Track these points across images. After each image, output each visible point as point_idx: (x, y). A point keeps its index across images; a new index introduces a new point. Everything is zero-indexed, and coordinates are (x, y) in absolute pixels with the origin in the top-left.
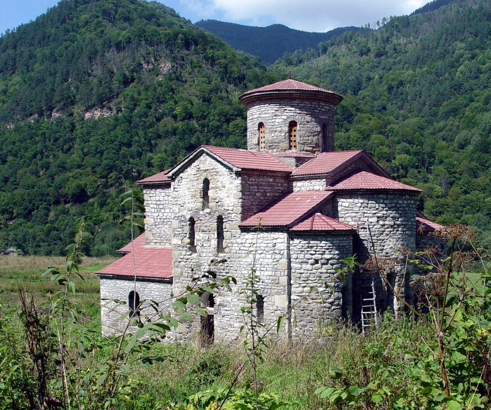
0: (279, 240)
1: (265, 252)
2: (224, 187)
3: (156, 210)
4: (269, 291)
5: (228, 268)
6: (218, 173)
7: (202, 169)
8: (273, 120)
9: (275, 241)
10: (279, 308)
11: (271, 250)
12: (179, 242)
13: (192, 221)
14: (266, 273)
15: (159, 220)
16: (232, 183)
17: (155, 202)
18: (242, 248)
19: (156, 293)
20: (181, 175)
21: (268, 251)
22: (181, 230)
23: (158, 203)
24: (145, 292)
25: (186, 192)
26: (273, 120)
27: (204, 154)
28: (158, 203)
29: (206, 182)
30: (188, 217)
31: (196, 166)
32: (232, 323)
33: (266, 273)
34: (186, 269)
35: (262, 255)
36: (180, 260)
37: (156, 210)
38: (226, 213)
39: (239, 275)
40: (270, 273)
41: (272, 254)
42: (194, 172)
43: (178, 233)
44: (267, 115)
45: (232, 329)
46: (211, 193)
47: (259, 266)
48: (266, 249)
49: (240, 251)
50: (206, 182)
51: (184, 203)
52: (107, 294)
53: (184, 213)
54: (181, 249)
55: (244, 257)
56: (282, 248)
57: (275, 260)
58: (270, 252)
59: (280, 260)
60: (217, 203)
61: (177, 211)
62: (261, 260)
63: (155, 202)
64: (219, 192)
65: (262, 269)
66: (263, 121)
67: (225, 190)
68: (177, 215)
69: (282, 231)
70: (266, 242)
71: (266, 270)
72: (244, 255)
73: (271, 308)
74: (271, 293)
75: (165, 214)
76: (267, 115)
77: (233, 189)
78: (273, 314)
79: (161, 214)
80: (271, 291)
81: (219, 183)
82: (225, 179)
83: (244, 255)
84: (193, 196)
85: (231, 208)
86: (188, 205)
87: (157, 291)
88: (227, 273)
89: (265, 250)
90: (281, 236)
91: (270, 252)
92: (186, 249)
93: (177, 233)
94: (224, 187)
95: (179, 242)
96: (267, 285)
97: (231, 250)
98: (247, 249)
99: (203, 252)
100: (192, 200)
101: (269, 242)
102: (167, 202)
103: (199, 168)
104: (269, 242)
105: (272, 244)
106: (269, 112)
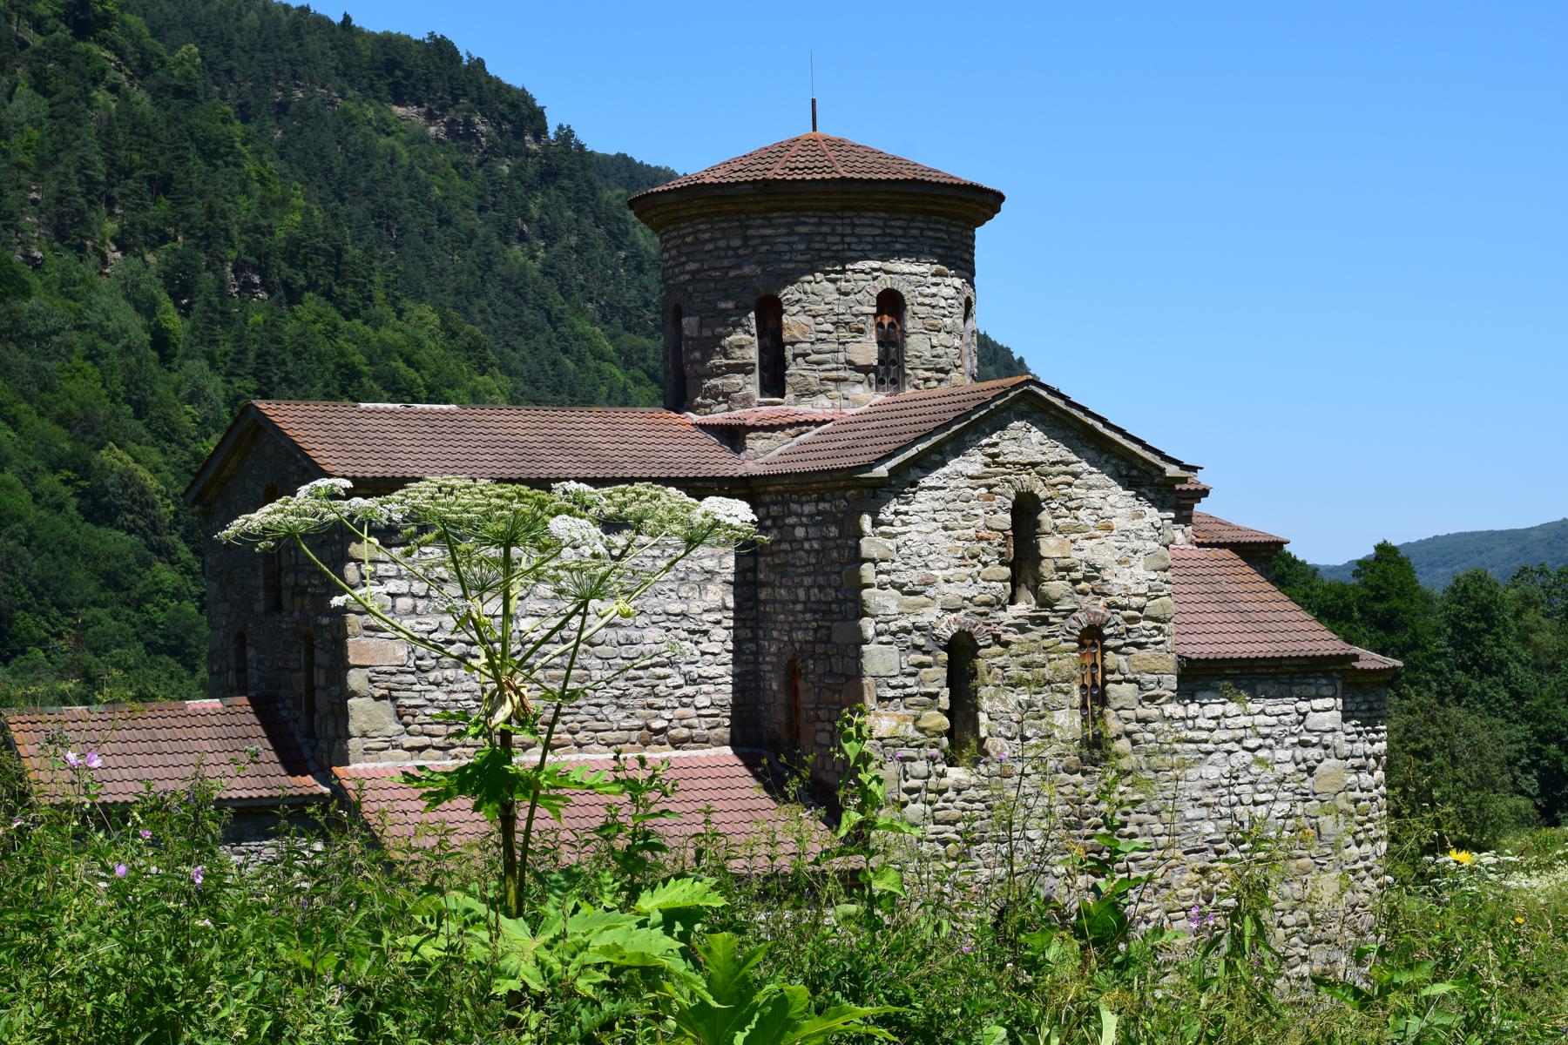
1: (1270, 741)
2: (1109, 528)
7: (1011, 458)
8: (934, 290)
13: (961, 654)
22: (910, 681)
25: (939, 537)
26: (934, 290)
30: (947, 627)
36: (904, 797)
46: (1049, 547)
47: (1249, 788)
50: (1026, 510)
53: (929, 615)
56: (1328, 726)
58: (1288, 741)
59: (1321, 767)
60: (1075, 582)
62: (1254, 769)
65: (1259, 797)
66: (903, 288)
68: (893, 627)
77: (1146, 534)
81: (1081, 514)
82: (1110, 499)
85: (1137, 601)
86: (945, 588)
91: (1288, 741)
93: (890, 693)
98: (1205, 735)
100: (968, 571)
103: (997, 455)
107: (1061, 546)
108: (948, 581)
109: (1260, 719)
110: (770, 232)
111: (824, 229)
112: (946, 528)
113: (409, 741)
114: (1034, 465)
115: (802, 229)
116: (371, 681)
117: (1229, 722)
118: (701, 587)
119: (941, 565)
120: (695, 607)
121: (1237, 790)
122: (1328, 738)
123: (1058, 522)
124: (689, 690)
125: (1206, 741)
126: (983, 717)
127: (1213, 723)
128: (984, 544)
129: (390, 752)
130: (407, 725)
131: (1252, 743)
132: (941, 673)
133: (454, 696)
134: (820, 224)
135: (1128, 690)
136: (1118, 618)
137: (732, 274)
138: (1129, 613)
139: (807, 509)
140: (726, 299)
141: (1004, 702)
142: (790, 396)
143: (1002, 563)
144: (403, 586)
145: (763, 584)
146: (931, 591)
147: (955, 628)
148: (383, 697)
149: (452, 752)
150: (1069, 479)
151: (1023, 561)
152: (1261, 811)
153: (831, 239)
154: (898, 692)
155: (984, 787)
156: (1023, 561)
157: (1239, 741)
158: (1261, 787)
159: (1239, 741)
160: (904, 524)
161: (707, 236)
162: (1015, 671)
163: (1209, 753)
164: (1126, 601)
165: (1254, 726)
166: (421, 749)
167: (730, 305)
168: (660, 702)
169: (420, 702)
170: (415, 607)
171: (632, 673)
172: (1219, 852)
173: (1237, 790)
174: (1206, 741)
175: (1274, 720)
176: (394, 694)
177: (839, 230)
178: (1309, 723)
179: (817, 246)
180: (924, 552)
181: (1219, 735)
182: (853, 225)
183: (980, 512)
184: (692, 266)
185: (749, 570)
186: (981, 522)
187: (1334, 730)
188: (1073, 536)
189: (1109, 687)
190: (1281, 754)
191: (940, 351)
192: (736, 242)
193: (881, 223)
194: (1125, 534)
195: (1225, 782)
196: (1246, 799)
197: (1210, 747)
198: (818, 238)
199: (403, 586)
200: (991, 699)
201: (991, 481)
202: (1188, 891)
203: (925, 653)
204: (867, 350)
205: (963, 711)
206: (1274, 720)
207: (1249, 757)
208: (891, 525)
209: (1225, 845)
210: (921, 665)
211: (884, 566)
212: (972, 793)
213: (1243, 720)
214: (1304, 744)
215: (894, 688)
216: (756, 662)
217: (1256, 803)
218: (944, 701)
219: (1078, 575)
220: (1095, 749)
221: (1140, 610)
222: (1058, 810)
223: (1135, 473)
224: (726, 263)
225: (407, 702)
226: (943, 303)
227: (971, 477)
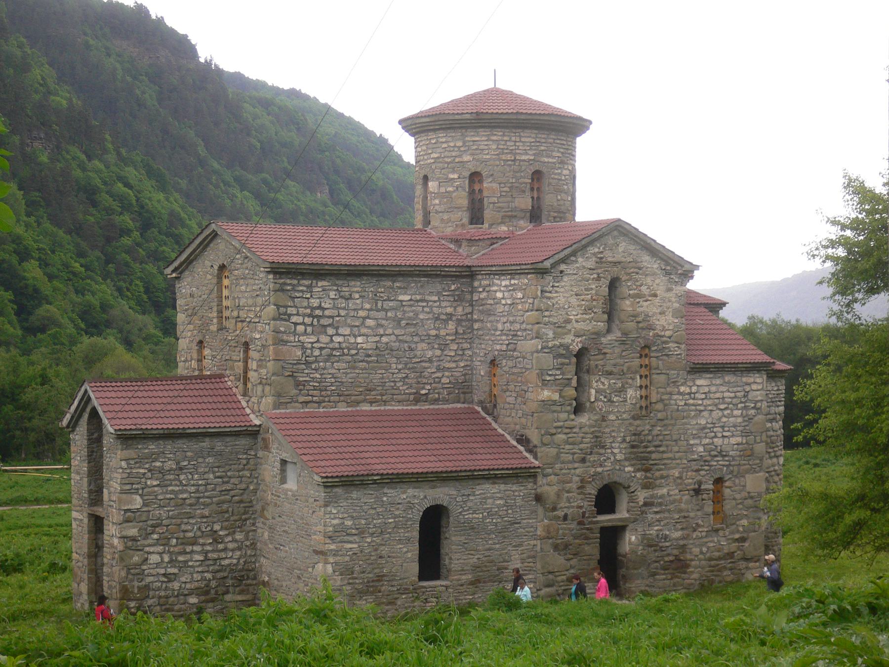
0: (754, 387)
1: (731, 406)
2: (655, 295)
3: (309, 329)
4: (736, 468)
5: (661, 438)
6: (640, 269)
7: (610, 259)
9: (748, 388)
10: (752, 494)
11: (741, 402)
12: (556, 396)
14: (733, 440)
15: (317, 353)
16: (669, 290)
17: (308, 311)
18: (691, 401)
19: (498, 502)
20: (563, 267)
21: (737, 405)
22: (558, 372)
23: (318, 312)
24: (469, 504)
25: (574, 301)
27: (616, 233)
28: (318, 312)
29: (613, 285)
30: (576, 347)
31: (594, 254)
32: (668, 533)
33: (733, 440)
34: (567, 447)
35: (726, 412)
36: (554, 431)
37: (309, 329)
38: (659, 342)
39: (683, 449)
40: (739, 439)
41: (742, 409)
42: (591, 264)
43: (552, 378)
44: (550, 160)
45: (667, 544)
46: (626, 305)
47: (721, 430)
48: (735, 401)
49: (687, 407)
51: (568, 321)
52: (349, 523)
53: (568, 339)
54: (559, 408)
55: (692, 418)
56: (759, 398)
57: (746, 419)
58: (740, 406)
59: (756, 418)
60: (638, 322)
61: (551, 335)
62: (724, 419)
63: (308, 311)
64: (645, 304)
65: (725, 434)
66: (544, 170)
67: (657, 300)
68: (550, 345)
69: (759, 371)
70: (735, 389)
71: (733, 436)
72: (693, 413)
73: (738, 496)
74: (738, 472)
75: (337, 339)
76: (550, 160)
77: (673, 300)
78: (741, 506)
79: (324, 339)
80: (739, 469)
81: (644, 288)
82: (657, 281)
83: (693, 413)
84: (588, 309)
85: (668, 333)
86: (576, 325)
87: (501, 498)
88: (656, 446)
89: (731, 403)
90: (758, 380)
91: (740, 406)
92: (569, 408)
93: (548, 378)
94: (655, 295)
95: (556, 396)
96: (734, 460)
97: (665, 405)
98: (700, 402)
99: (609, 413)
100: (587, 317)
101: (739, 389)
102: (343, 313)
103: (601, 258)
104: (739, 389)
105: (742, 393)
106: (555, 154)
107: (632, 305)
108: (577, 321)
109: (726, 394)
110: (477, 139)
111: (505, 138)
112: (577, 295)
113: (302, 399)
114: (619, 263)
115: (494, 138)
116: (283, 367)
117: (712, 395)
118: (446, 321)
119: (574, 313)
120: (443, 332)
121: (715, 430)
122: (759, 404)
123: (631, 292)
124: (439, 375)
125: (699, 405)
126: (593, 392)
127: (703, 396)
128: (594, 303)
129: (293, 404)
130: (301, 390)
131: (722, 407)
132: (573, 368)
133: (324, 376)
134: (504, 135)
135: (663, 378)
136: (659, 342)
137: (457, 160)
138: (665, 339)
139: (504, 283)
140: (454, 172)
141: (603, 383)
142: (486, 225)
143: (603, 312)
144: (299, 319)
145: (476, 321)
146: (569, 327)
147: (580, 346)
148: (289, 376)
149: (323, 404)
150: (636, 270)
151: (611, 312)
152: (726, 441)
153: (508, 143)
154: (552, 378)
155: (594, 427)
156: (611, 312)
157: (716, 405)
158: (726, 429)
159: (716, 405)
160: (556, 292)
161: (444, 140)
162: (608, 368)
163: (701, 411)
164: (663, 333)
165: (723, 398)
166: (307, 403)
167: (456, 176)
168: (425, 381)
169: (307, 379)
170: (306, 330)
171: (411, 366)
172: (705, 461)
173: (715, 430)
174: (699, 405)
175: (732, 395)
176: (295, 374)
177: (513, 139)
178: (750, 397)
179: (502, 147)
180: (566, 307)
181: (706, 402)
182: (520, 137)
183: (594, 287)
184: (435, 155)
185: (469, 313)
186: (594, 292)
187: (762, 401)
188: (638, 300)
189: (654, 376)
190: (736, 412)
191: (562, 202)
192: (459, 144)
193: (533, 135)
194: (663, 300)
195: (709, 426)
196: (720, 435)
197: (702, 408)
198: (503, 143)
199: (299, 319)
200: (597, 382)
201: (599, 271)
202: (690, 481)
203: (565, 358)
204: (525, 202)
205: (581, 386)
206: (732, 395)
207: (720, 414)
208: (550, 292)
209: (708, 458)
210: (563, 364)
211: (547, 313)
212: (586, 429)
213: (718, 395)
214: (745, 408)
215: (550, 375)
216: (472, 361)
217: (723, 436)
218: (574, 383)
219: (640, 319)
220: (645, 408)
221: (670, 337)
222: (628, 439)
223: (668, 268)
224: (454, 154)
225: (301, 379)
226: (563, 178)
227: (590, 269)
